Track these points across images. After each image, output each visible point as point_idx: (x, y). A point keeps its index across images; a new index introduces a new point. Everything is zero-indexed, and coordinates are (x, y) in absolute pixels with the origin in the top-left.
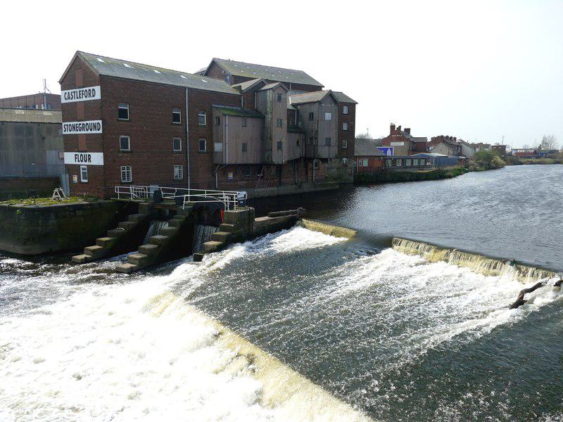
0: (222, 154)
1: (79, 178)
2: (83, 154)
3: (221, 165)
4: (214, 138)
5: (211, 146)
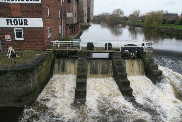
0: (72, 19)
1: (13, 37)
2: (18, 19)
3: (71, 24)
4: (67, 10)
5: (66, 15)
